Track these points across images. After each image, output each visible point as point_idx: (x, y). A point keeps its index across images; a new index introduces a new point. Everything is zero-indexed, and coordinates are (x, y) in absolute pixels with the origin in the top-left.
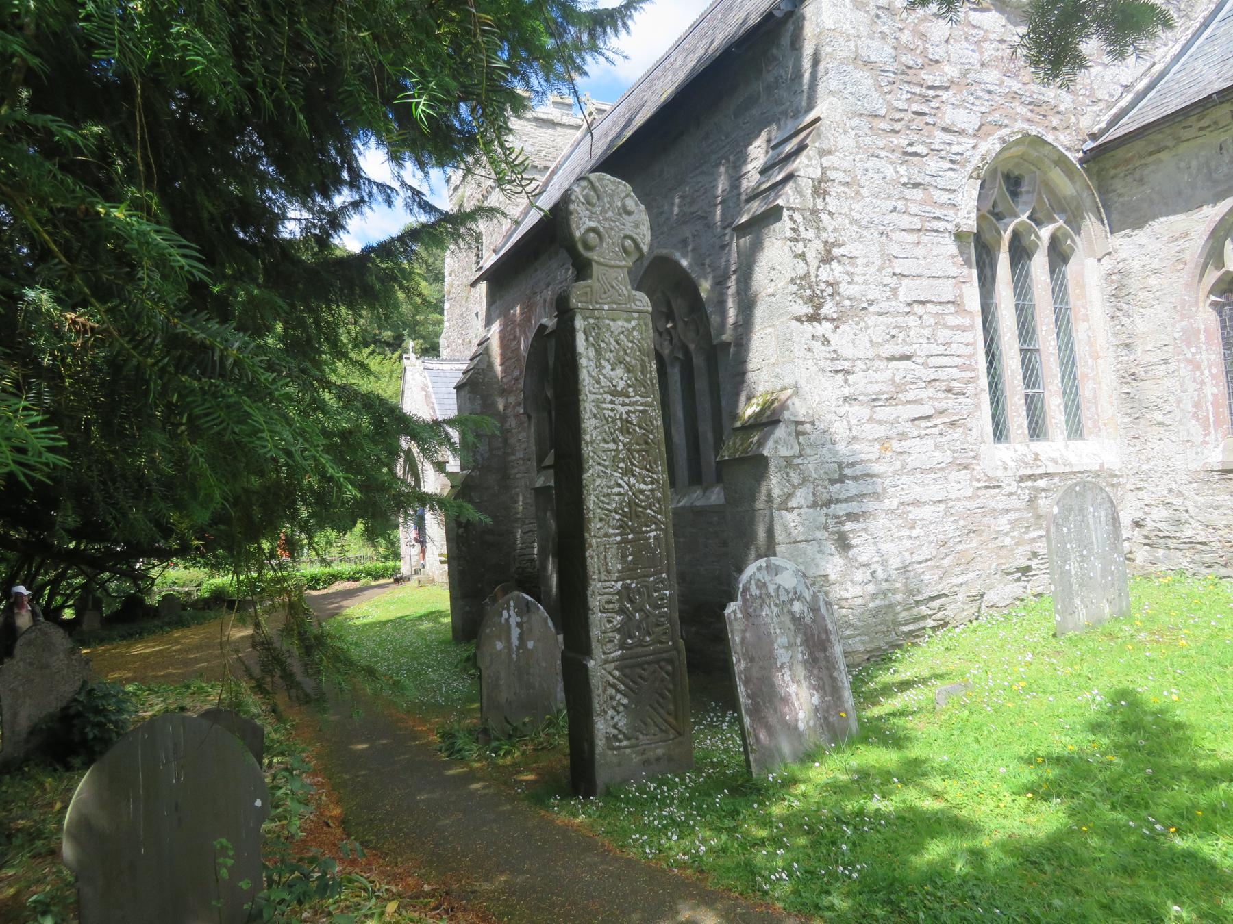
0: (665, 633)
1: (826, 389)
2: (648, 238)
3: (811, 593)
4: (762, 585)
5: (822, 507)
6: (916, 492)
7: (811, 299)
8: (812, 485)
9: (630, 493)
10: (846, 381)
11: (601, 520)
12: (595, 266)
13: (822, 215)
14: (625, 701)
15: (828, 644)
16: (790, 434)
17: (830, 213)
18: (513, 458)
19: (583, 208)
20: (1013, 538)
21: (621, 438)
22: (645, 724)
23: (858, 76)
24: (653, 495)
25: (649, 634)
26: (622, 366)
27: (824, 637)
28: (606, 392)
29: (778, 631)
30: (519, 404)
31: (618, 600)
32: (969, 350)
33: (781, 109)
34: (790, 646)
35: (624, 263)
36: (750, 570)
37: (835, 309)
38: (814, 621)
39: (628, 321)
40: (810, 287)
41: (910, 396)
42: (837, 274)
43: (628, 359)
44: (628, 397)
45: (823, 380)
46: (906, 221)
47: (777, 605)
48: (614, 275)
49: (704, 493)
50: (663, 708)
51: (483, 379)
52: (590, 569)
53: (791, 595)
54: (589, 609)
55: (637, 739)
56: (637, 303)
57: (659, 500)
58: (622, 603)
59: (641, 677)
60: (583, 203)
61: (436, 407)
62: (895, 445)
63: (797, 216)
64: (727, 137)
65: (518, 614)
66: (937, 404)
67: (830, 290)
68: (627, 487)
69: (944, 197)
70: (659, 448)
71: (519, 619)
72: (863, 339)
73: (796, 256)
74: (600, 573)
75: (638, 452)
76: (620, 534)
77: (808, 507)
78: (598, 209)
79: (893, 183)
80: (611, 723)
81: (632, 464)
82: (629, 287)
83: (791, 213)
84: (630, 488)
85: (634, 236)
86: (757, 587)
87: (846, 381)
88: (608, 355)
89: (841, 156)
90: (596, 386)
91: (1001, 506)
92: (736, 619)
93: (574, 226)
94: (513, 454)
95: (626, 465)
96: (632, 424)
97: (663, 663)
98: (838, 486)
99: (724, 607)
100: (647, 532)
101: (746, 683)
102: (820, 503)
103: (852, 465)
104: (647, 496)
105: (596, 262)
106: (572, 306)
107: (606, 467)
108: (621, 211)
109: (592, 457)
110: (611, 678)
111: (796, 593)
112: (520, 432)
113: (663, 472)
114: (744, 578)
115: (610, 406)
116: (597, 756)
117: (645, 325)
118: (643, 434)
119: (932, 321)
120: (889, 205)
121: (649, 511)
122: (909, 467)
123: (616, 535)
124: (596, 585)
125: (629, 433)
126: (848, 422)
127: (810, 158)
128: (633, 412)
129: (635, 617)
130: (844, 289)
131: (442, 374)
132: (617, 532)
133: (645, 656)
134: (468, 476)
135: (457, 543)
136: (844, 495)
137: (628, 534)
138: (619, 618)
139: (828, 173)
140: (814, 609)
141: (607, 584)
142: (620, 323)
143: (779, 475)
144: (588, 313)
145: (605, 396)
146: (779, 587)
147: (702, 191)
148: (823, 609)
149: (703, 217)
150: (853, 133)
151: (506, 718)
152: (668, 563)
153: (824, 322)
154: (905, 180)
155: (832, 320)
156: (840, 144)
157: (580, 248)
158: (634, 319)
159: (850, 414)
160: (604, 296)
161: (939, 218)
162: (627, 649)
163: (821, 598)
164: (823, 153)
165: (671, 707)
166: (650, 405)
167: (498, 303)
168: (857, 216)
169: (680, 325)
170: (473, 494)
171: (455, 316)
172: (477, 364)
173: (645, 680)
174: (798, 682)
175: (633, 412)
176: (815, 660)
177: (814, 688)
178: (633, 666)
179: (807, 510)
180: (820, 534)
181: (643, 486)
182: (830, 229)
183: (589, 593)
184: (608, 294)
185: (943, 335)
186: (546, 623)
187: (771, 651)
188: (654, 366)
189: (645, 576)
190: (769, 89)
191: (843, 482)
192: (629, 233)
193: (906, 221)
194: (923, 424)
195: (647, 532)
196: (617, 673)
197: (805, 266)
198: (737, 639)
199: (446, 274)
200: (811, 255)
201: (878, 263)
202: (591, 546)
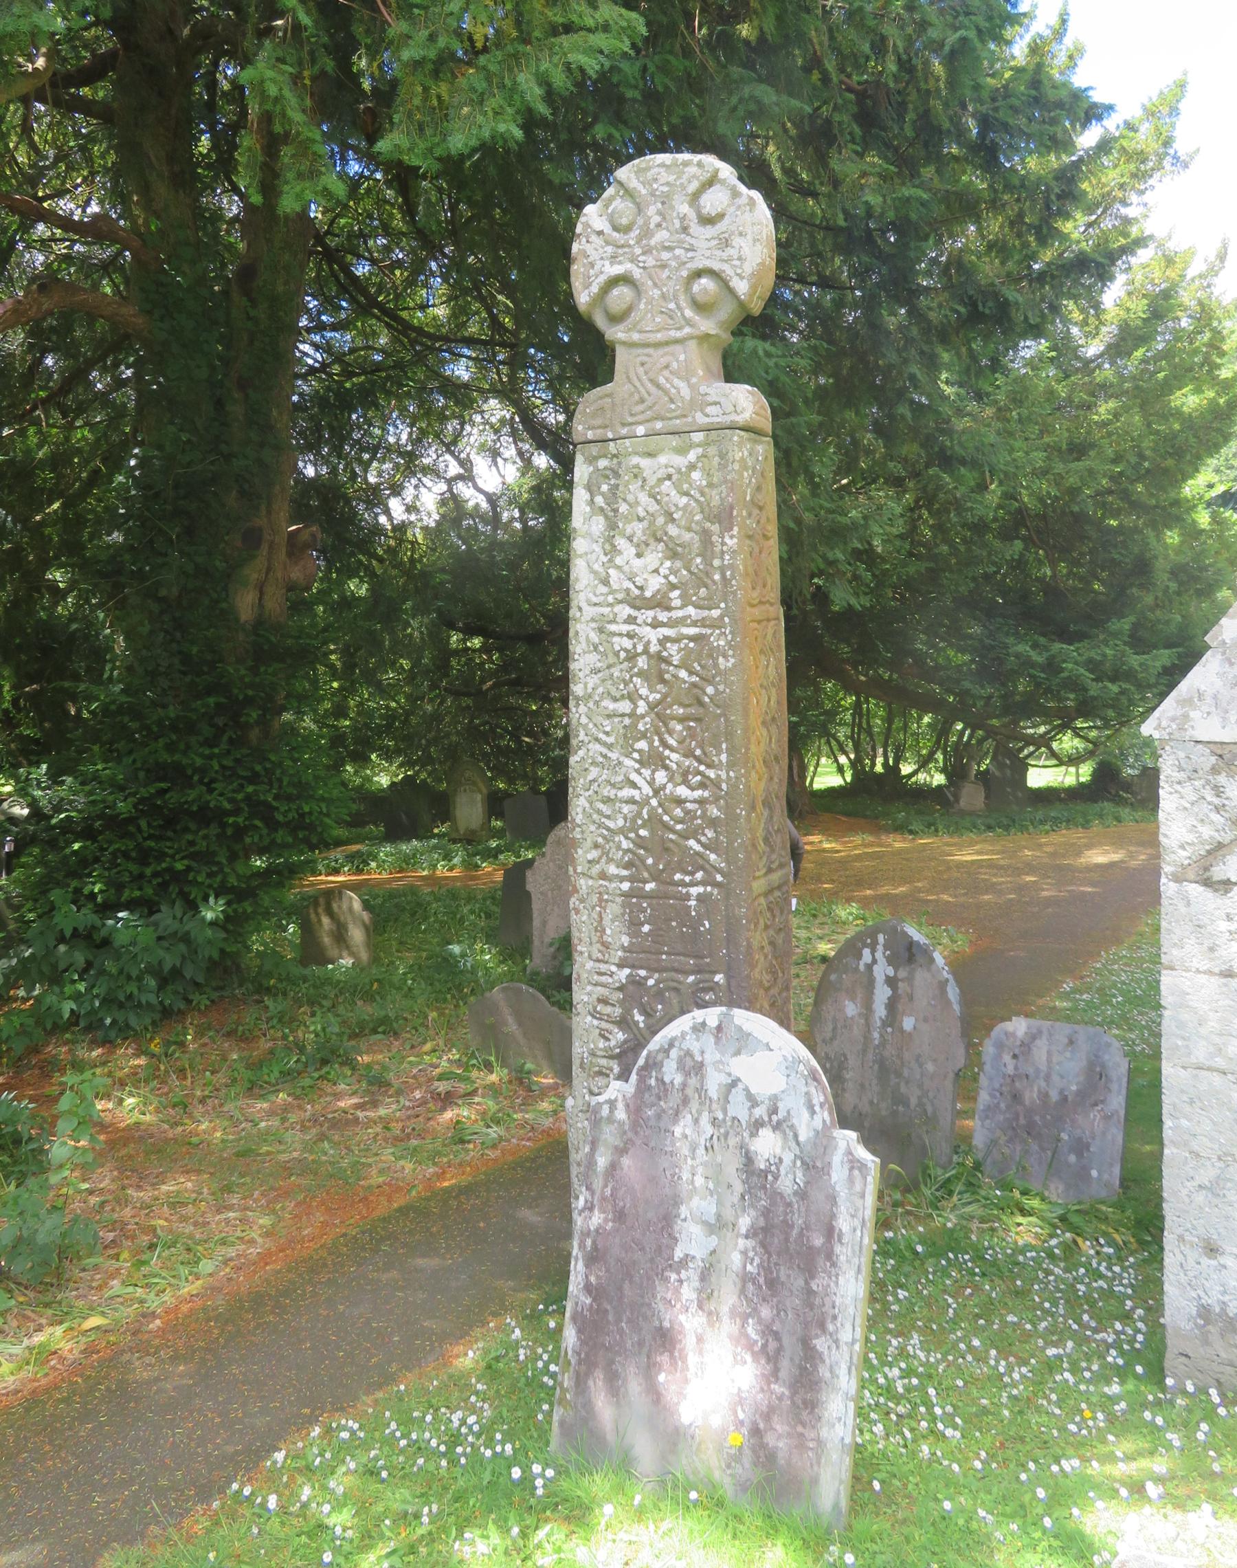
4: (694, 1068)
9: (654, 802)
11: (596, 846)
12: (621, 356)
21: (644, 691)
26: (661, 546)
27: (818, 1241)
28: (621, 602)
34: (717, 1226)
35: (687, 330)
36: (682, 1024)
38: (802, 1195)
39: (682, 451)
43: (673, 530)
44: (669, 609)
47: (714, 1122)
48: (664, 361)
53: (760, 1112)
57: (713, 823)
60: (600, 233)
65: (890, 961)
68: (647, 790)
75: (682, 720)
76: (631, 879)
84: (656, 792)
90: (603, 589)
92: (610, 1120)
93: (577, 284)
95: (651, 743)
96: (670, 664)
100: (682, 883)
101: (592, 1259)
104: (687, 812)
105: (624, 343)
107: (610, 747)
111: (774, 1111)
113: (731, 765)
115: (625, 628)
118: (694, 685)
121: (692, 843)
123: (622, 879)
125: (663, 681)
128: (676, 641)
132: (625, 873)
137: (645, 882)
138: (621, 1036)
141: (604, 968)
142: (663, 459)
144: (594, 449)
145: (617, 609)
146: (734, 1083)
157: (600, 321)
158: (692, 446)
160: (640, 408)
163: (842, 1145)
166: (716, 624)
174: (713, 1317)
175: (676, 641)
177: (750, 1346)
181: (683, 791)
189: (677, 971)
195: (685, 885)
202: (576, 891)
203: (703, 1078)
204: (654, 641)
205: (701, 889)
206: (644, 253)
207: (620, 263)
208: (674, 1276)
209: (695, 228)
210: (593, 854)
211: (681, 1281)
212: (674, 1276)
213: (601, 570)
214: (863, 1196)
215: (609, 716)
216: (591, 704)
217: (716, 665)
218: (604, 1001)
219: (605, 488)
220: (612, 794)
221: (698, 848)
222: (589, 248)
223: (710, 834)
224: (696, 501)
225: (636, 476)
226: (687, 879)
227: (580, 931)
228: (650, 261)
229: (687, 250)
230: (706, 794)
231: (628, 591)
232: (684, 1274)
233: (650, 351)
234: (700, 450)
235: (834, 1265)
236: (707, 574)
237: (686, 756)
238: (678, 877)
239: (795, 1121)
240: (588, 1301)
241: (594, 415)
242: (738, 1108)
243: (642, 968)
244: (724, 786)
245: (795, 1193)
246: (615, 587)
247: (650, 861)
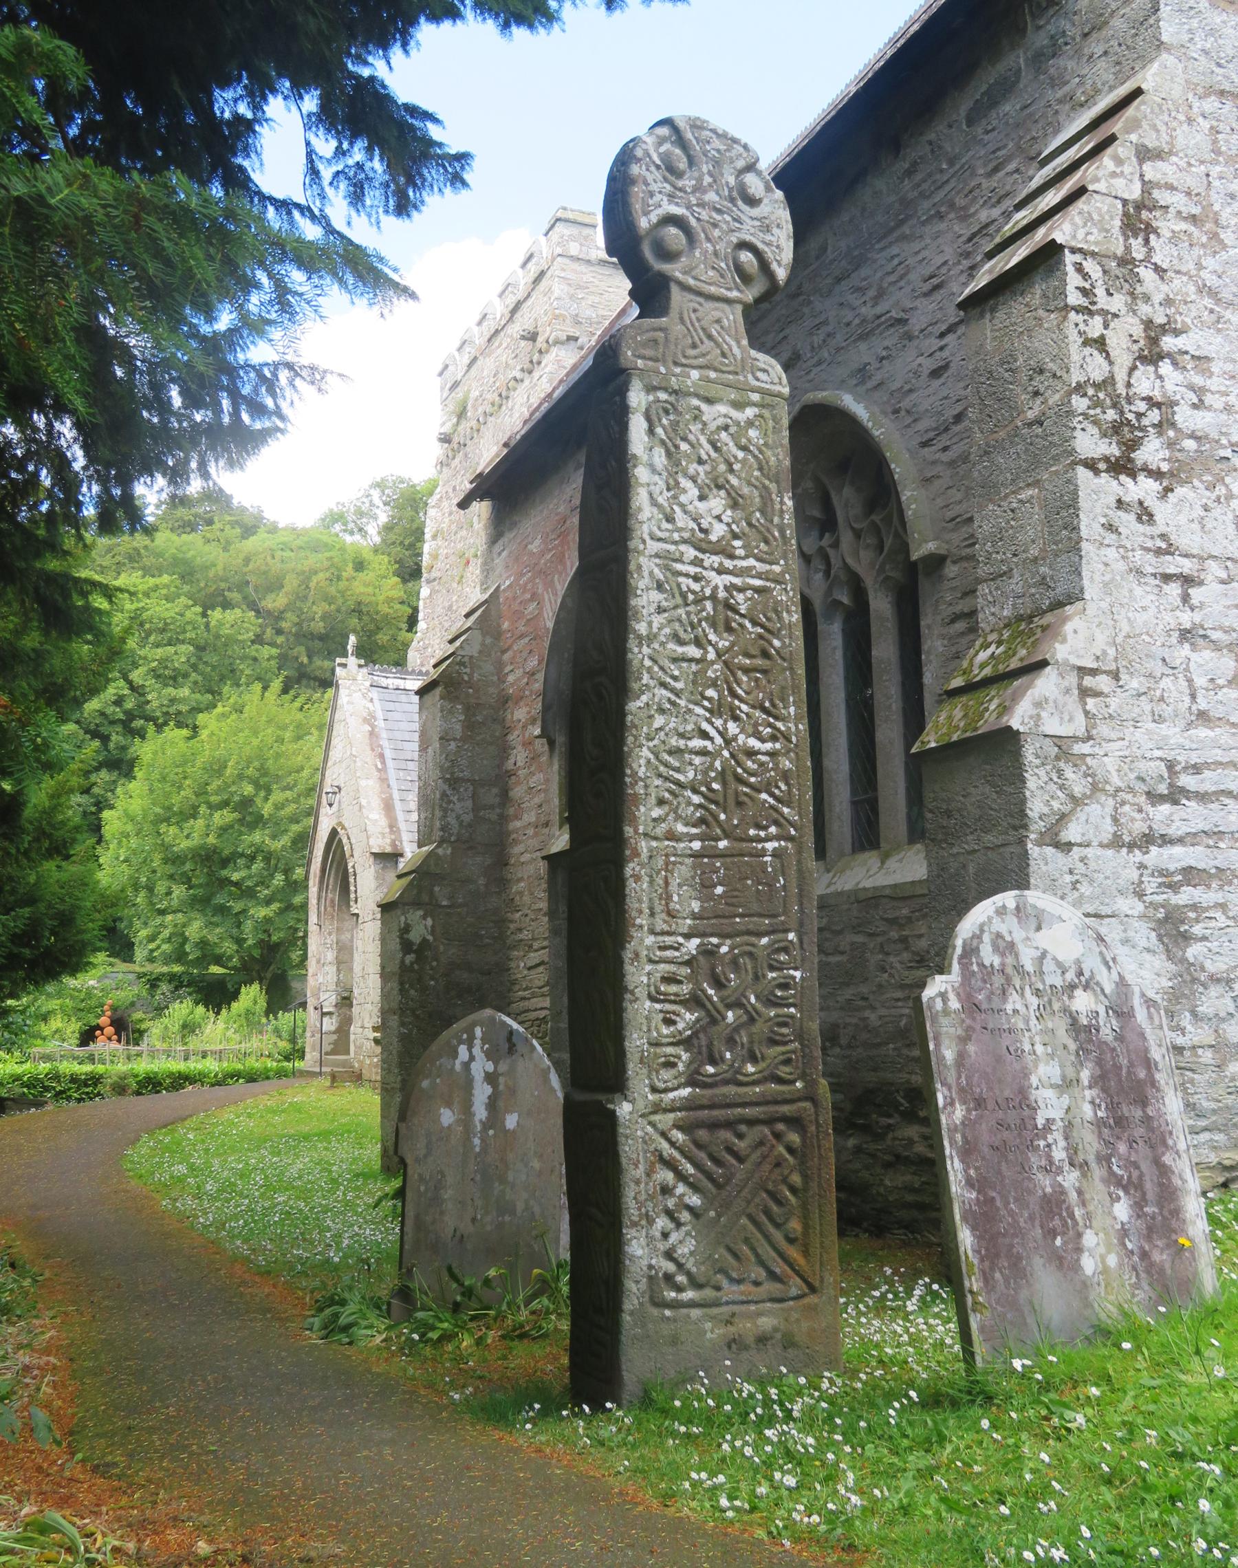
0: (787, 1062)
1: (1144, 609)
2: (787, 255)
3: (1115, 977)
4: (1006, 947)
5: (1131, 846)
7: (1116, 429)
8: (1111, 802)
9: (726, 753)
10: (1186, 598)
11: (661, 802)
12: (676, 293)
13: (1141, 270)
14: (695, 1200)
15: (1150, 1092)
16: (1067, 691)
17: (1158, 269)
18: (518, 824)
19: (658, 175)
21: (712, 637)
22: (736, 1256)
23: (1218, 21)
24: (776, 764)
25: (754, 1059)
26: (723, 493)
27: (1142, 1074)
28: (685, 541)
29: (1039, 1049)
30: (533, 721)
31: (689, 978)
33: (1060, 94)
34: (1067, 1084)
35: (734, 294)
36: (981, 912)
37: (1167, 454)
38: (1120, 1038)
39: (739, 405)
40: (1114, 406)
42: (1170, 387)
43: (734, 481)
44: (732, 557)
45: (1138, 591)
47: (1038, 993)
48: (717, 314)
49: (883, 863)
50: (778, 1226)
51: (471, 675)
52: (632, 904)
53: (1070, 976)
54: (626, 989)
55: (718, 1288)
56: (760, 375)
57: (786, 776)
58: (697, 984)
59: (730, 1150)
61: (388, 754)
63: (1090, 266)
64: (951, 163)
67: (1154, 416)
68: (719, 740)
70: (791, 669)
71: (490, 1067)
73: (1087, 342)
74: (652, 914)
75: (746, 671)
77: (1101, 845)
78: (688, 183)
80: (662, 1246)
81: (734, 695)
82: (745, 342)
83: (1078, 258)
84: (728, 742)
85: (760, 246)
86: (996, 949)
87: (1186, 598)
88: (693, 468)
89: (1182, 164)
90: (665, 525)
92: (946, 1012)
93: (637, 207)
94: (517, 817)
95: (720, 693)
96: (737, 612)
97: (781, 1127)
98: (1165, 808)
99: (922, 985)
101: (967, 1153)
102: (1127, 839)
103: (1196, 769)
104: (762, 764)
106: (623, 363)
107: (677, 693)
108: (735, 194)
109: (649, 670)
110: (665, 1145)
111: (1080, 973)
112: (532, 774)
113: (798, 719)
114: (966, 927)
115: (692, 570)
116: (626, 1318)
117: (774, 419)
118: (761, 637)
121: (764, 796)
123: (692, 838)
124: (642, 941)
125: (729, 629)
127: (1119, 161)
129: (724, 1018)
130: (1184, 416)
131: (403, 698)
132: (694, 831)
133: (744, 1105)
134: (430, 854)
135: (402, 984)
136: (1177, 830)
137: (718, 839)
138: (689, 1017)
139: (1156, 194)
140: (1122, 1012)
141: (669, 940)
142: (722, 409)
143: (1041, 772)
145: (683, 548)
146: (1044, 954)
147: (901, 271)
148: (1141, 1015)
149: (902, 322)
150: (1205, 125)
151: (450, 1269)
152: (801, 910)
153: (1141, 478)
155: (1157, 474)
156: (1180, 142)
159: (1192, 665)
162: (704, 1086)
163: (1137, 990)
164: (1145, 154)
165: (795, 1225)
167: (509, 536)
168: (1211, 280)
169: (847, 538)
170: (437, 889)
171: (439, 610)
172: (461, 647)
173: (741, 1160)
176: (1120, 1122)
178: (713, 1126)
179: (1100, 851)
181: (753, 743)
182: (1157, 298)
183: (628, 955)
184: (702, 349)
186: (547, 1080)
187: (1023, 1092)
188: (790, 503)
189: (749, 933)
190: (1039, 60)
191: (1176, 802)
192: (748, 238)
195: (760, 840)
196: (679, 1136)
197: (1105, 364)
198: (949, 1055)
199: (427, 536)
200: (1118, 342)
203: (1017, 956)
204: (721, 588)
205: (776, 844)
206: (698, 205)
207: (677, 204)
208: (1042, 1143)
209: (740, 203)
210: (657, 812)
211: (1049, 1146)
212: (1042, 1143)
213: (666, 504)
214: (1161, 1028)
215: (675, 660)
216: (656, 646)
217: (780, 618)
218: (669, 979)
219: (665, 421)
220: (682, 743)
221: (771, 800)
222: (650, 178)
223: (783, 787)
224: (755, 457)
225: (696, 418)
226: (762, 834)
227: (640, 901)
228: (704, 215)
229: (735, 220)
230: (778, 746)
231: (692, 530)
232: (1050, 1139)
233: (701, 300)
234: (756, 410)
235: (1158, 1090)
236: (768, 530)
237: (753, 707)
238: (752, 832)
239: (1098, 978)
240: (974, 1195)
241: (645, 344)
243: (712, 935)
244: (794, 739)
245: (1116, 1039)
246: (680, 524)
247: (723, 817)
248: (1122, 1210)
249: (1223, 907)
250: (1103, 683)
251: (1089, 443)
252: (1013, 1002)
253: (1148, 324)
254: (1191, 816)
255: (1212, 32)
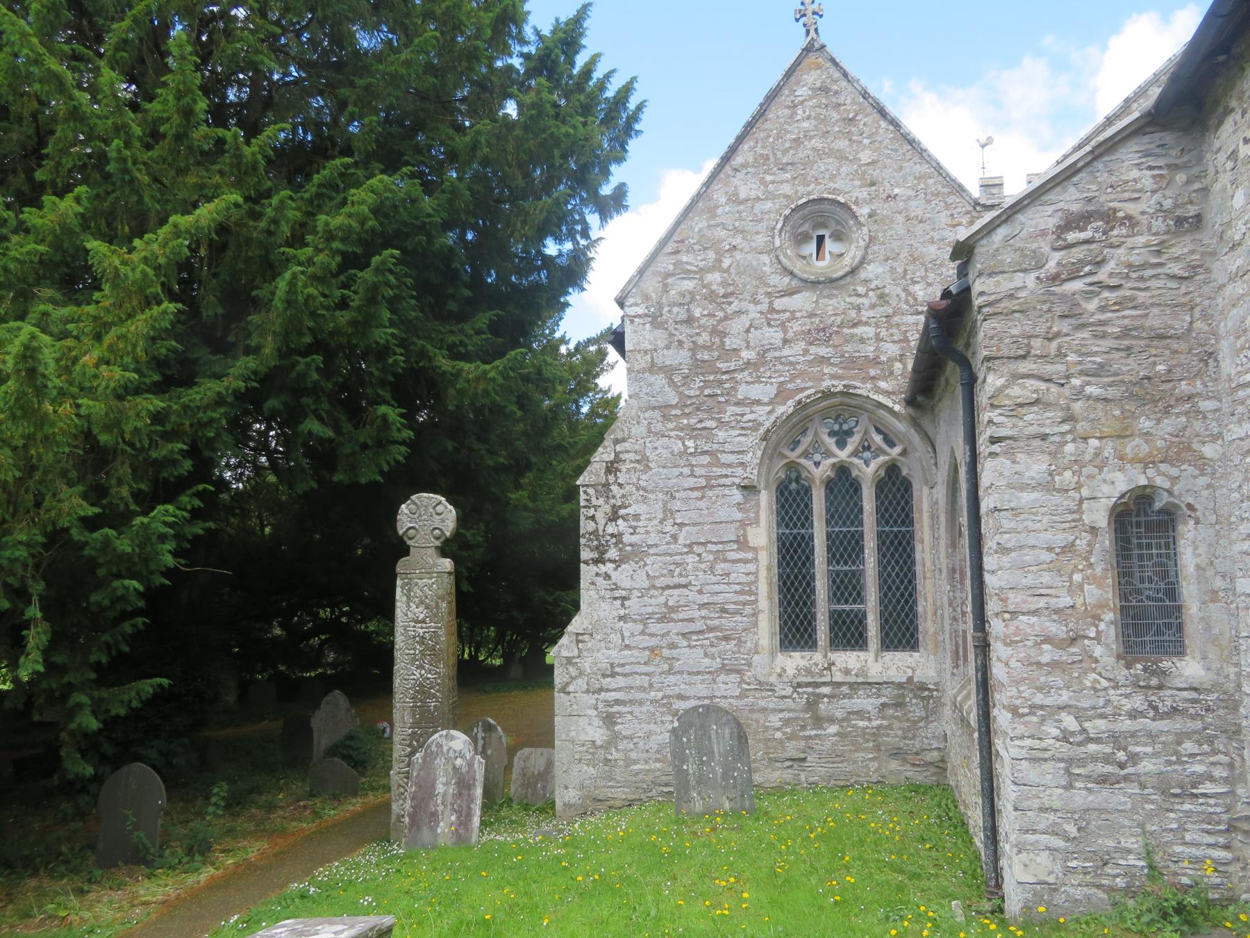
4: (440, 746)
6: (683, 689)
7: (597, 548)
10: (623, 605)
12: (412, 550)
13: (612, 487)
17: (620, 485)
20: (784, 734)
32: (751, 578)
41: (681, 616)
42: (621, 528)
46: (691, 482)
62: (666, 652)
63: (591, 491)
66: (709, 622)
69: (732, 458)
72: (641, 575)
73: (587, 518)
79: (681, 454)
87: (623, 605)
91: (771, 706)
101: (412, 799)
103: (623, 665)
119: (711, 557)
120: (676, 471)
122: (676, 669)
126: (622, 635)
130: (627, 538)
136: (613, 686)
150: (645, 422)
154: (692, 450)
161: (726, 476)
180: (589, 712)
185: (721, 567)
193: (691, 482)
194: (695, 637)
201: (660, 516)
242: (452, 754)
248: (453, 818)
249: (631, 713)
250: (586, 637)
251: (585, 554)
252: (438, 761)
253: (614, 506)
254: (620, 681)
255: (650, 385)
